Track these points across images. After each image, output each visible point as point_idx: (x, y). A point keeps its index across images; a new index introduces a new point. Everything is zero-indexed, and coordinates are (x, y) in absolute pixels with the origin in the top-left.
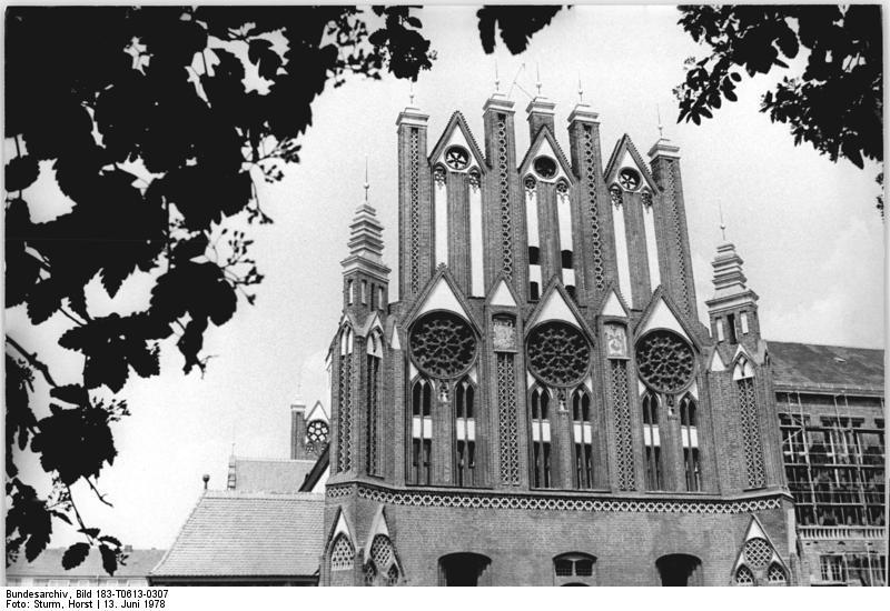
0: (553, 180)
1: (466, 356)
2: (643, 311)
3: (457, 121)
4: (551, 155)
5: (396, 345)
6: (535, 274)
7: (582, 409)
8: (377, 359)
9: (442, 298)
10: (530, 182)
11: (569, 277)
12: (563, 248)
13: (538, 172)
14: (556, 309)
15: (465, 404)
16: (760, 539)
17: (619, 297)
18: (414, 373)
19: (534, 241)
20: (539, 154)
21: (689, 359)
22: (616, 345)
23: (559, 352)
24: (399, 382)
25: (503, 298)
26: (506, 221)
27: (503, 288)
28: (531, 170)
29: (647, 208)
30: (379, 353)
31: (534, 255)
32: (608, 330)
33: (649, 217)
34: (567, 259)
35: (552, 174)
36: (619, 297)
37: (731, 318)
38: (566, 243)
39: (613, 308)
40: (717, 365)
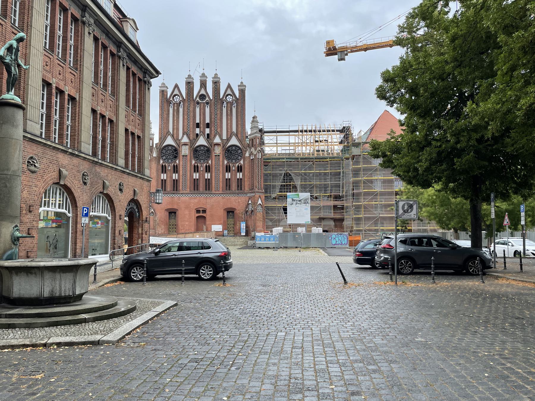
2: (228, 140)
3: (176, 86)
4: (205, 94)
5: (155, 155)
6: (198, 131)
7: (208, 169)
9: (170, 141)
10: (198, 103)
11: (207, 131)
14: (202, 141)
15: (176, 169)
18: (161, 162)
19: (198, 121)
20: (200, 93)
22: (218, 150)
23: (201, 153)
26: (189, 115)
28: (198, 99)
31: (198, 125)
32: (216, 146)
33: (234, 110)
34: (208, 126)
35: (205, 99)
39: (217, 140)
40: (247, 155)
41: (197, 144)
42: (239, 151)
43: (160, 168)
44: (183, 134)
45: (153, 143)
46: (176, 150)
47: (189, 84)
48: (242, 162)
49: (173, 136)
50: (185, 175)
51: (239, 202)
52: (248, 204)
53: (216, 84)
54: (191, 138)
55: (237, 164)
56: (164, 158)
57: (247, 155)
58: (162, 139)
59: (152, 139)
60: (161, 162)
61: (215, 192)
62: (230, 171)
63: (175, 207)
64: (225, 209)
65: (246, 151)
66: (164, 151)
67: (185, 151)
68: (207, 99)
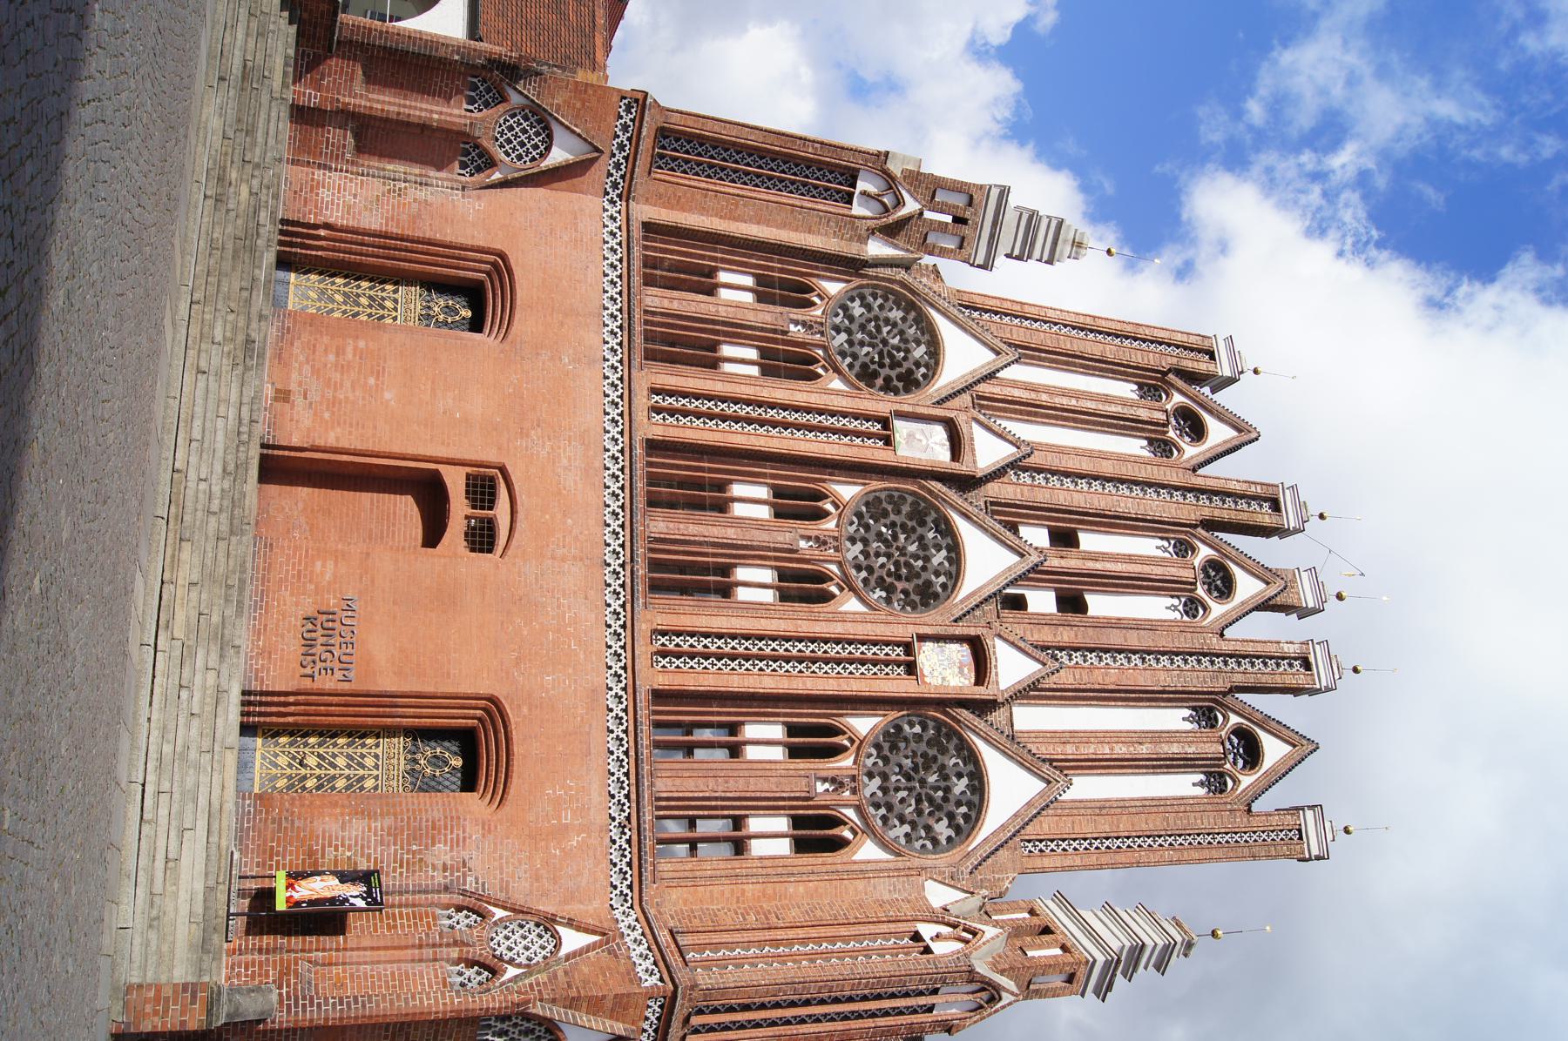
0: (1201, 591)
1: (867, 375)
2: (1017, 748)
5: (876, 248)
6: (1036, 536)
7: (802, 585)
8: (848, 199)
9: (962, 356)
10: (1184, 549)
11: (1042, 601)
12: (1089, 598)
13: (1204, 569)
16: (558, 946)
17: (1031, 692)
19: (1089, 541)
21: (935, 842)
22: (944, 669)
24: (815, 242)
25: (987, 451)
27: (1004, 452)
28: (1204, 552)
29: (1202, 784)
30: (858, 209)
31: (1064, 539)
34: (1072, 603)
36: (1031, 692)
37: (1046, 930)
38: (1099, 605)
40: (939, 895)
41: (963, 527)
42: (942, 829)
43: (793, 270)
44: (1016, 443)
45: (943, 253)
46: (910, 383)
47: (1264, 511)
48: (868, 851)
49: (990, 376)
50: (760, 412)
51: (563, 831)
52: (547, 924)
53: (1297, 673)
54: (993, 489)
55: (850, 813)
56: (857, 310)
57: (939, 895)
58: (971, 310)
59: (961, 250)
60: (833, 288)
61: (643, 628)
62: (795, 752)
63: (524, 324)
64: (494, 709)
65: (951, 881)
66: (896, 314)
67: (923, 445)
68: (1217, 609)
